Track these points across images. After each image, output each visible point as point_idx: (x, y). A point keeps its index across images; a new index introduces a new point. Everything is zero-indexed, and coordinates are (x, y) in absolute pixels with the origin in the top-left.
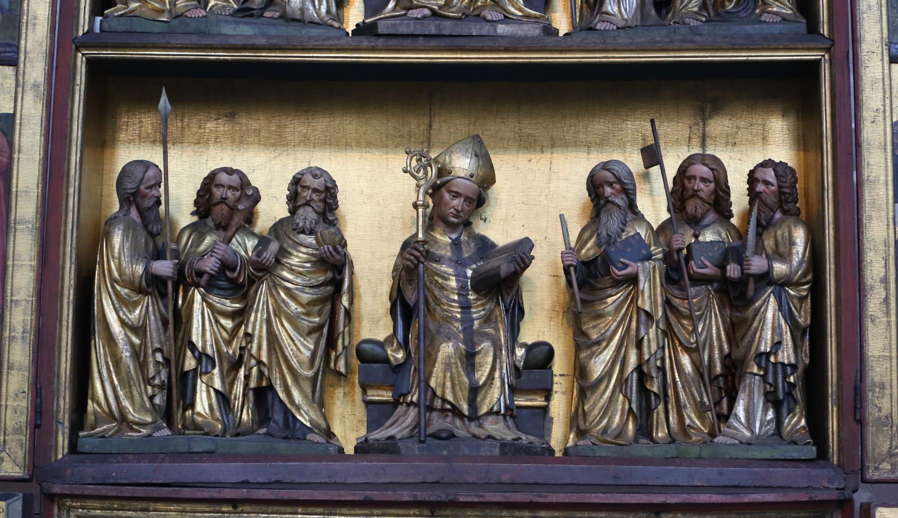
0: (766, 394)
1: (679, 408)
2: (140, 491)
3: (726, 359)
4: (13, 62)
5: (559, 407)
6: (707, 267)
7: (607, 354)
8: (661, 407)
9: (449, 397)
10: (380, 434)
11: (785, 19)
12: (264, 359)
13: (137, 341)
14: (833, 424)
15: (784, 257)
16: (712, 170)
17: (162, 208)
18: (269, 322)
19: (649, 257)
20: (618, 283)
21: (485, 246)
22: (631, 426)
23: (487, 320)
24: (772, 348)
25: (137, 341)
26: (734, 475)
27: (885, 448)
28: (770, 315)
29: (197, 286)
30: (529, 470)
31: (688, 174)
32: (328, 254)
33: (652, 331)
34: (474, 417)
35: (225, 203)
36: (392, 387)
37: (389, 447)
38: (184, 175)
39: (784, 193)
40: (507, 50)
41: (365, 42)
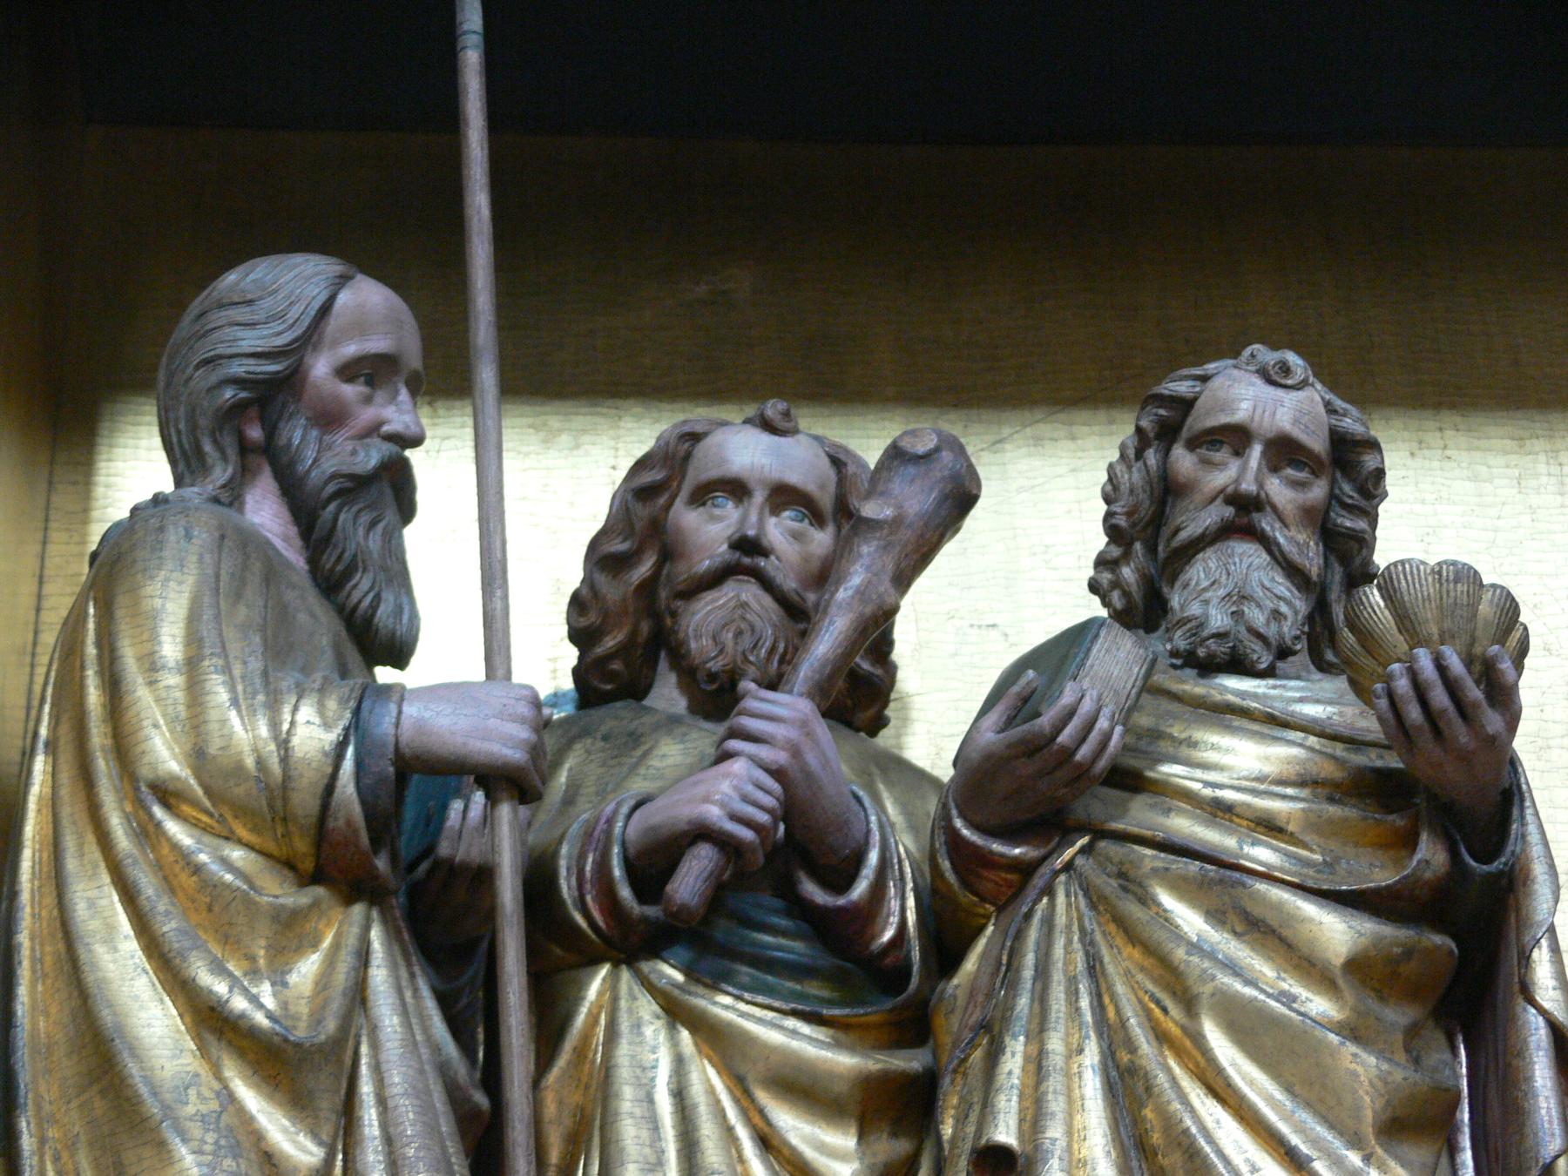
18: (1127, 1089)
29: (630, 945)
32: (1440, 697)
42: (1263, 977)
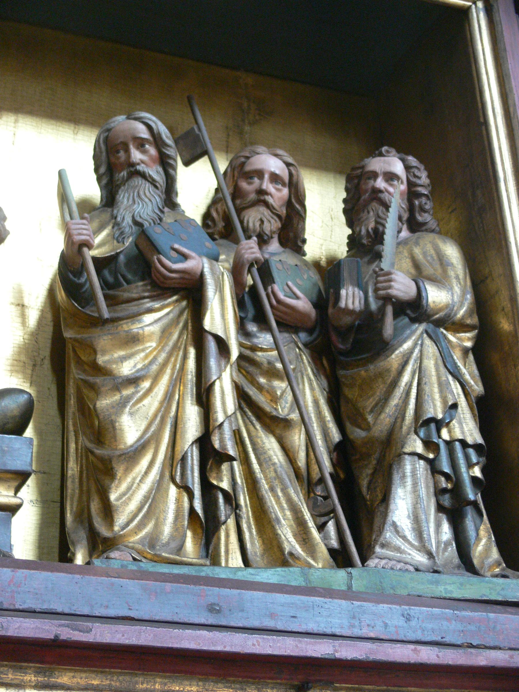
0: (439, 492)
6: (297, 298)
8: (231, 522)
15: (440, 281)
16: (288, 165)
24: (444, 413)
31: (248, 168)
39: (419, 195)
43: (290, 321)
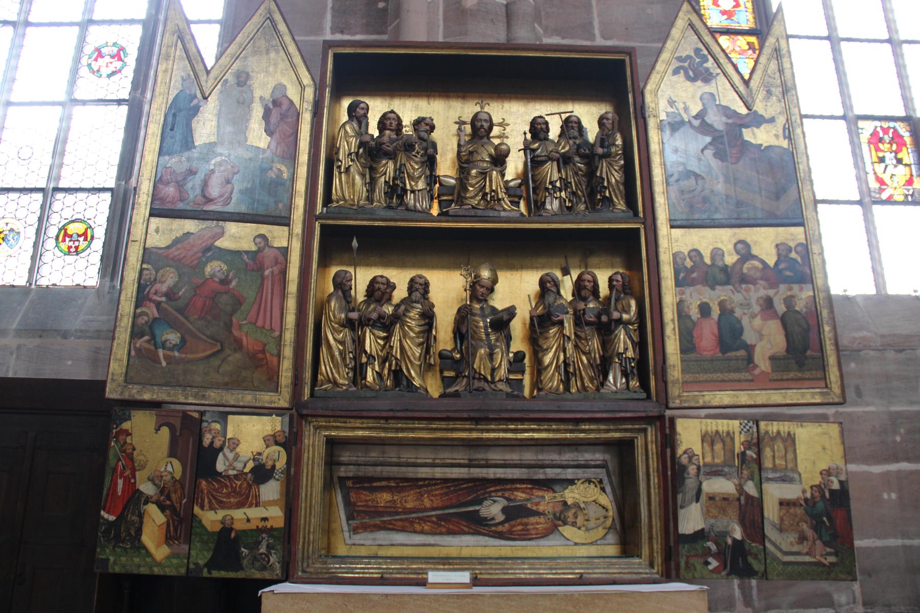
0: (622, 371)
1: (582, 379)
2: (343, 413)
3: (601, 357)
4: (288, 225)
5: (527, 379)
7: (551, 355)
9: (483, 373)
10: (451, 390)
11: (623, 211)
12: (399, 357)
13: (341, 348)
14: (653, 383)
15: (628, 312)
17: (353, 292)
19: (567, 313)
20: (554, 324)
21: (494, 309)
22: (561, 386)
23: (497, 340)
25: (341, 348)
26: (611, 406)
27: (677, 393)
28: (622, 337)
29: (368, 325)
30: (519, 404)
33: (570, 345)
34: (493, 382)
35: (379, 291)
36: (454, 370)
37: (456, 395)
38: (362, 279)
40: (505, 222)
41: (443, 218)
42: (412, 334)
43: (588, 324)
